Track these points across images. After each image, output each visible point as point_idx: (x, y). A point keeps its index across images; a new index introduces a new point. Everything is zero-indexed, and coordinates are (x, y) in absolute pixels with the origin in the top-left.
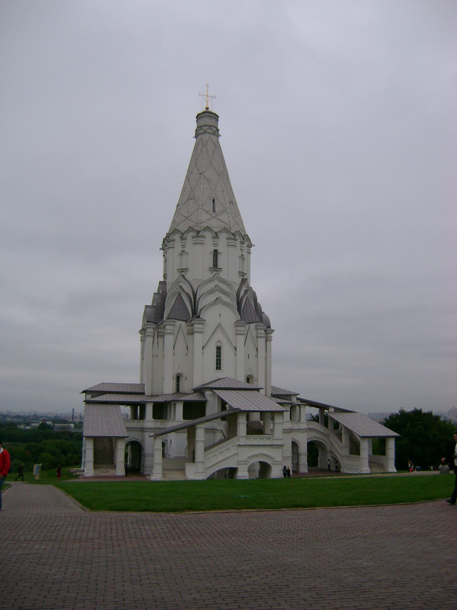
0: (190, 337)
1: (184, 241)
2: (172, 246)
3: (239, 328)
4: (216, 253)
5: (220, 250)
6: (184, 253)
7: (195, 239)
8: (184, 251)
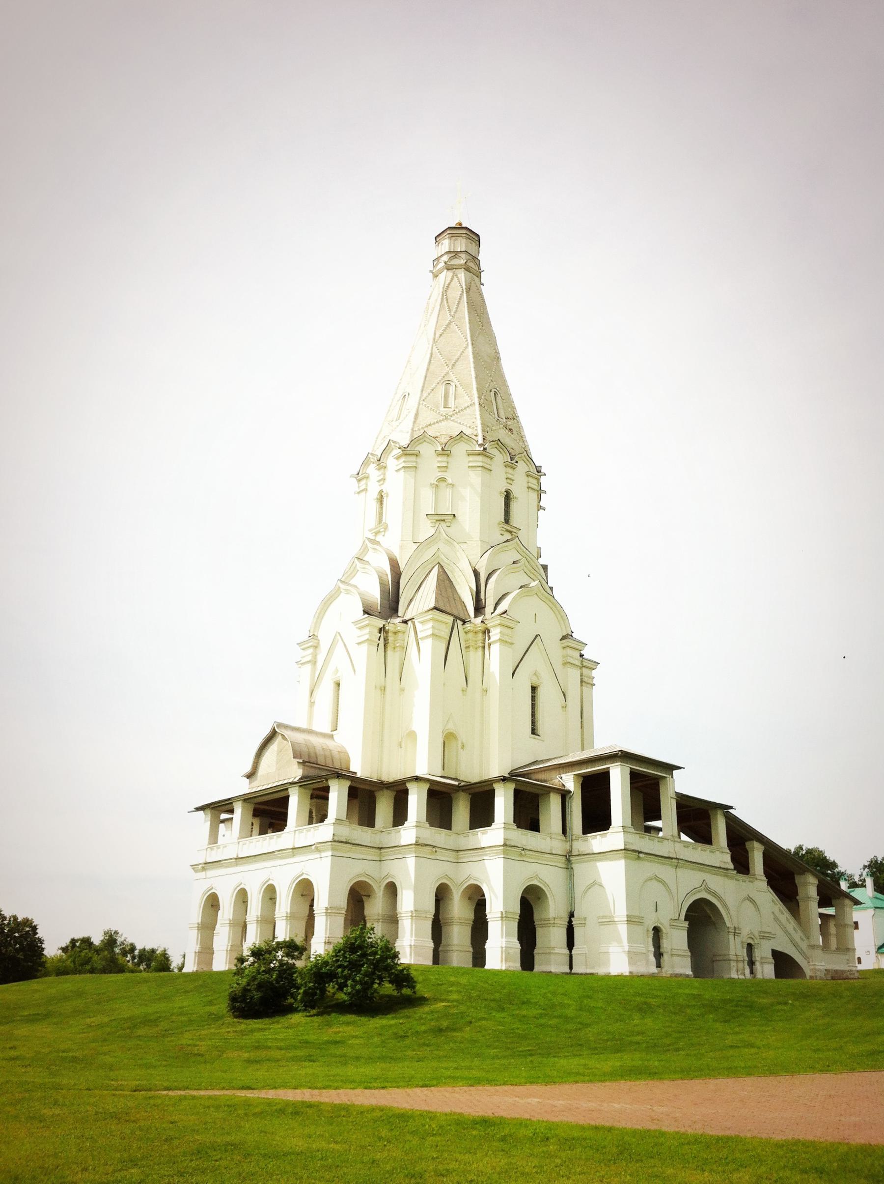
0: (475, 657)
1: (444, 458)
2: (414, 464)
3: (570, 652)
4: (508, 498)
5: (516, 492)
6: (442, 485)
7: (471, 458)
8: (442, 479)
